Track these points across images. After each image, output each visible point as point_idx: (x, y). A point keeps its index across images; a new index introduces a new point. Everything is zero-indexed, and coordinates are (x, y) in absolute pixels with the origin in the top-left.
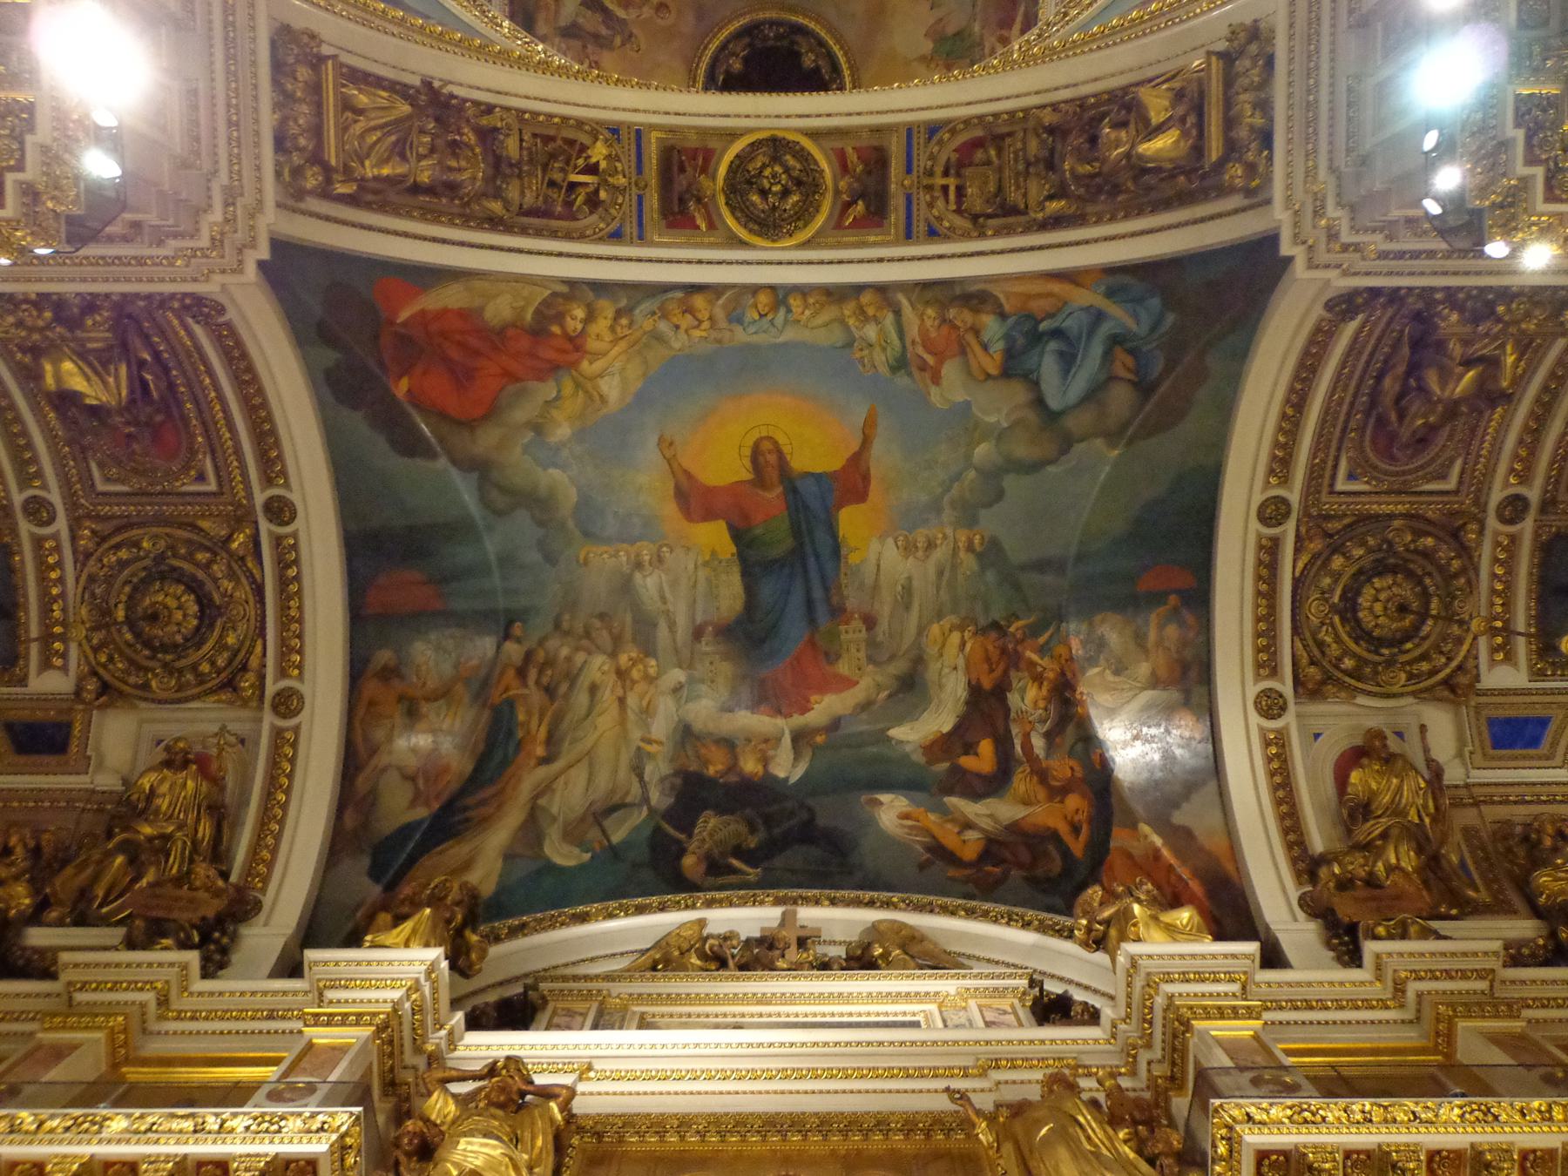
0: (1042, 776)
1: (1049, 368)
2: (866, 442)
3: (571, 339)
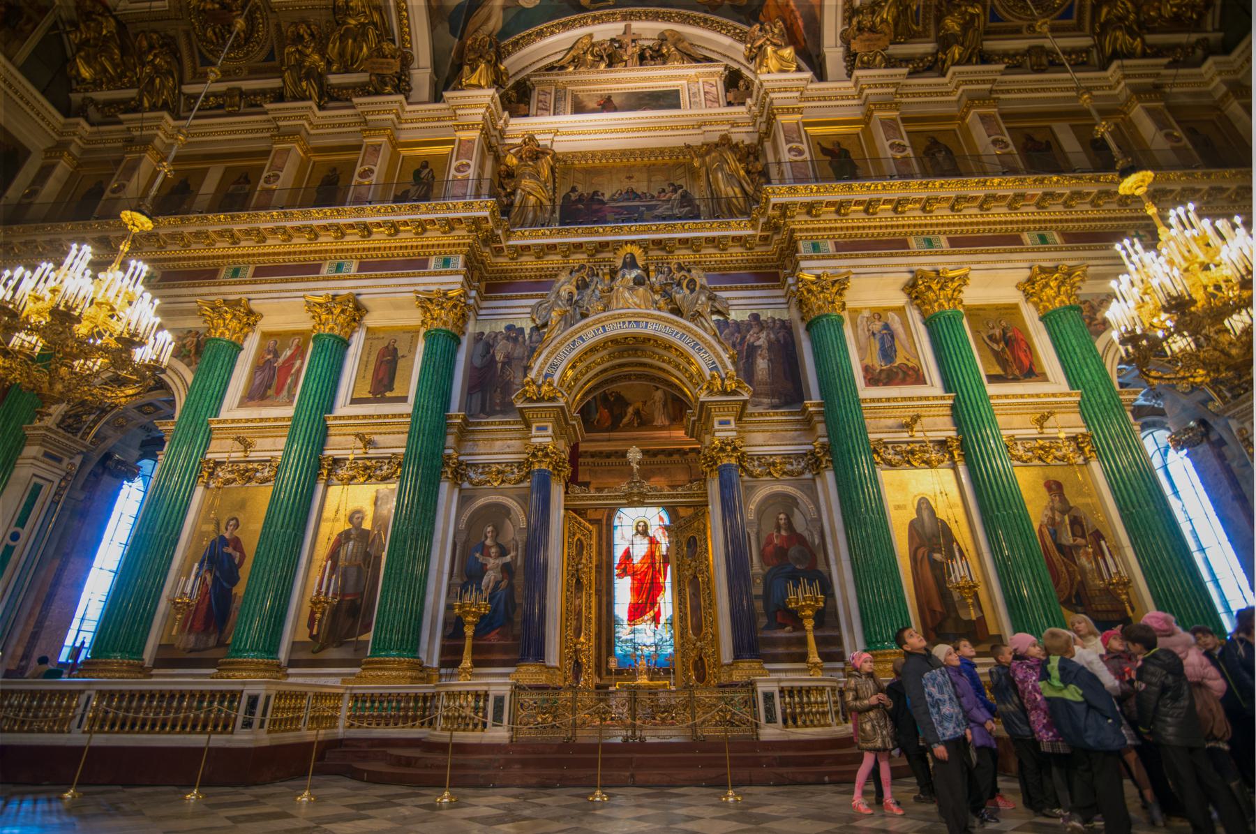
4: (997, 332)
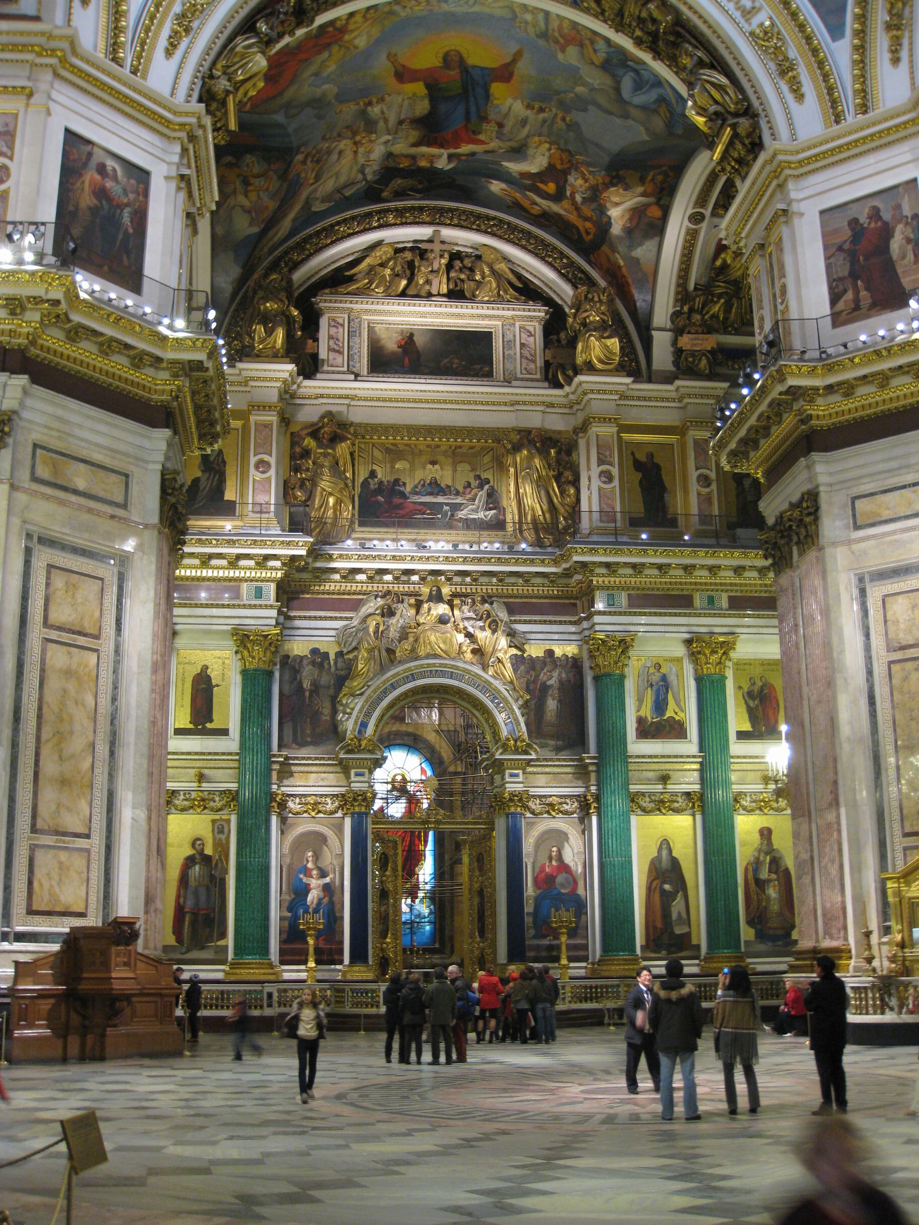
0: (577, 209)
1: (627, 83)
2: (514, 61)
3: (336, 29)
4: (756, 689)
